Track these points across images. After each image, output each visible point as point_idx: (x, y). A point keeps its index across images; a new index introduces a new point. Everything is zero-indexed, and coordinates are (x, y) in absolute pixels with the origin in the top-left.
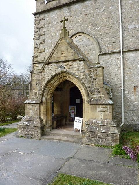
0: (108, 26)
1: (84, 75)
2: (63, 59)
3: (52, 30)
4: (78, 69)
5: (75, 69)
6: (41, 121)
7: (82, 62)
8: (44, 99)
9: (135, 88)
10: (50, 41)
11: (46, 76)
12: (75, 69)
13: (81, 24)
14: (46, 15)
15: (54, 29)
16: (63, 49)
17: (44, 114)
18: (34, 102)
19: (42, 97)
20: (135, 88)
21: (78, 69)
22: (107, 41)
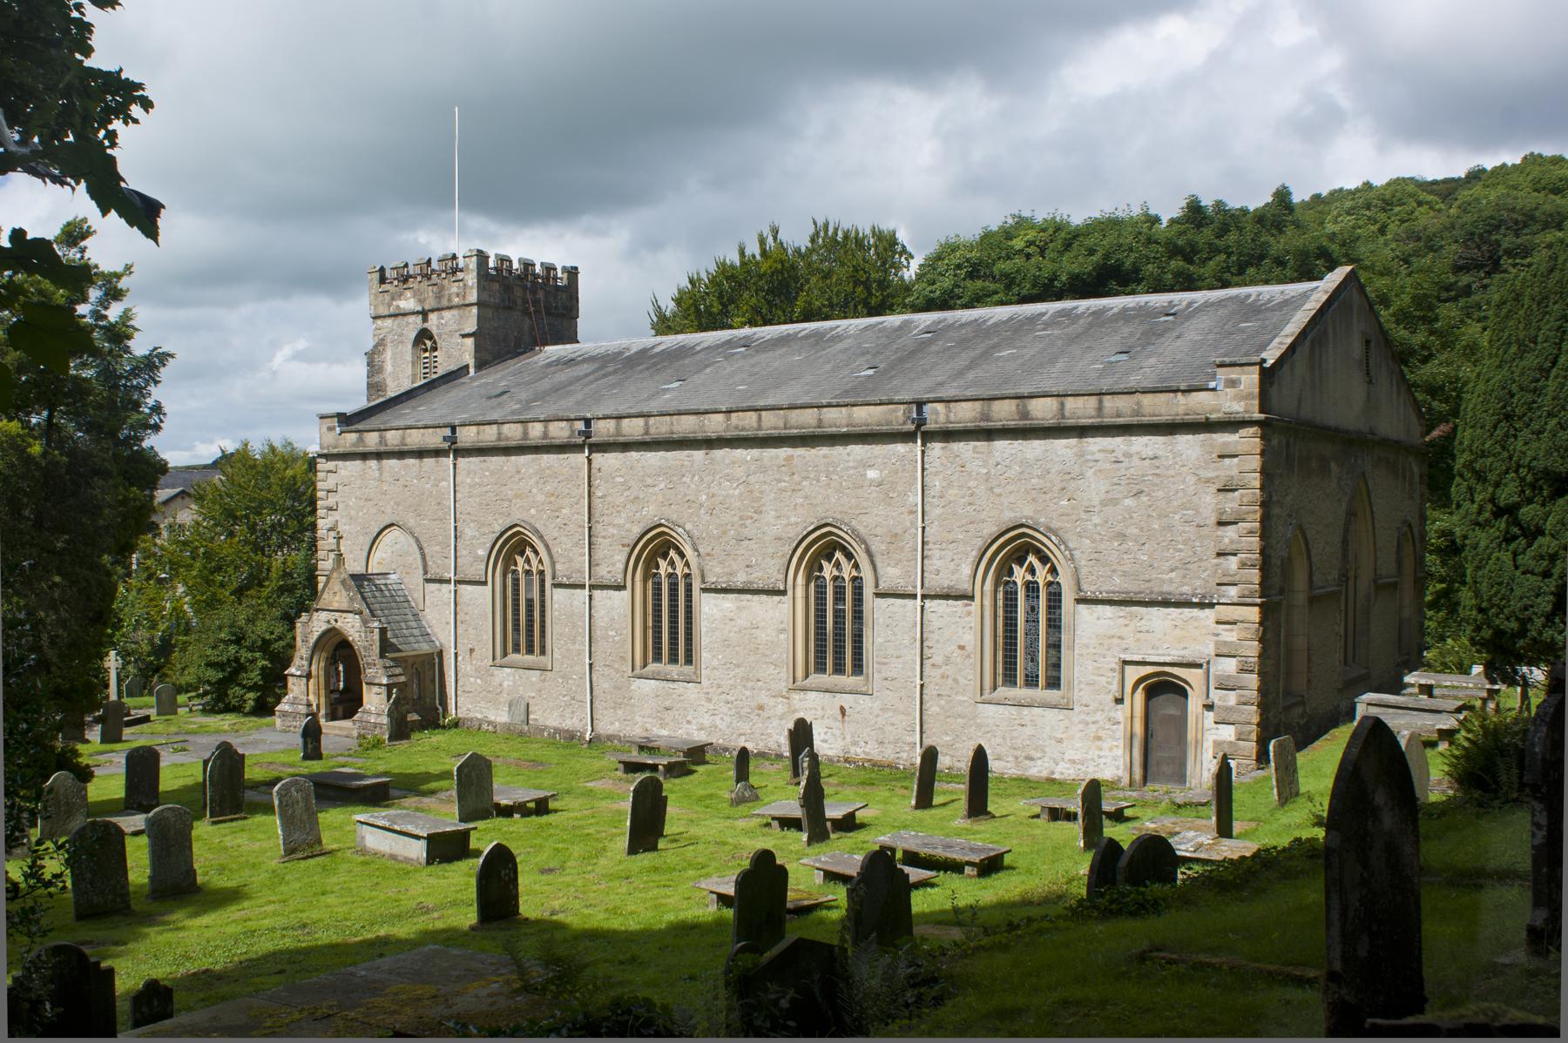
0: (438, 522)
1: (360, 636)
4: (353, 627)
5: (350, 625)
6: (309, 705)
7: (357, 616)
8: (314, 668)
9: (472, 650)
11: (314, 629)
12: (350, 625)
13: (398, 504)
17: (314, 693)
19: (310, 664)
20: (472, 650)
21: (353, 627)
22: (437, 552)
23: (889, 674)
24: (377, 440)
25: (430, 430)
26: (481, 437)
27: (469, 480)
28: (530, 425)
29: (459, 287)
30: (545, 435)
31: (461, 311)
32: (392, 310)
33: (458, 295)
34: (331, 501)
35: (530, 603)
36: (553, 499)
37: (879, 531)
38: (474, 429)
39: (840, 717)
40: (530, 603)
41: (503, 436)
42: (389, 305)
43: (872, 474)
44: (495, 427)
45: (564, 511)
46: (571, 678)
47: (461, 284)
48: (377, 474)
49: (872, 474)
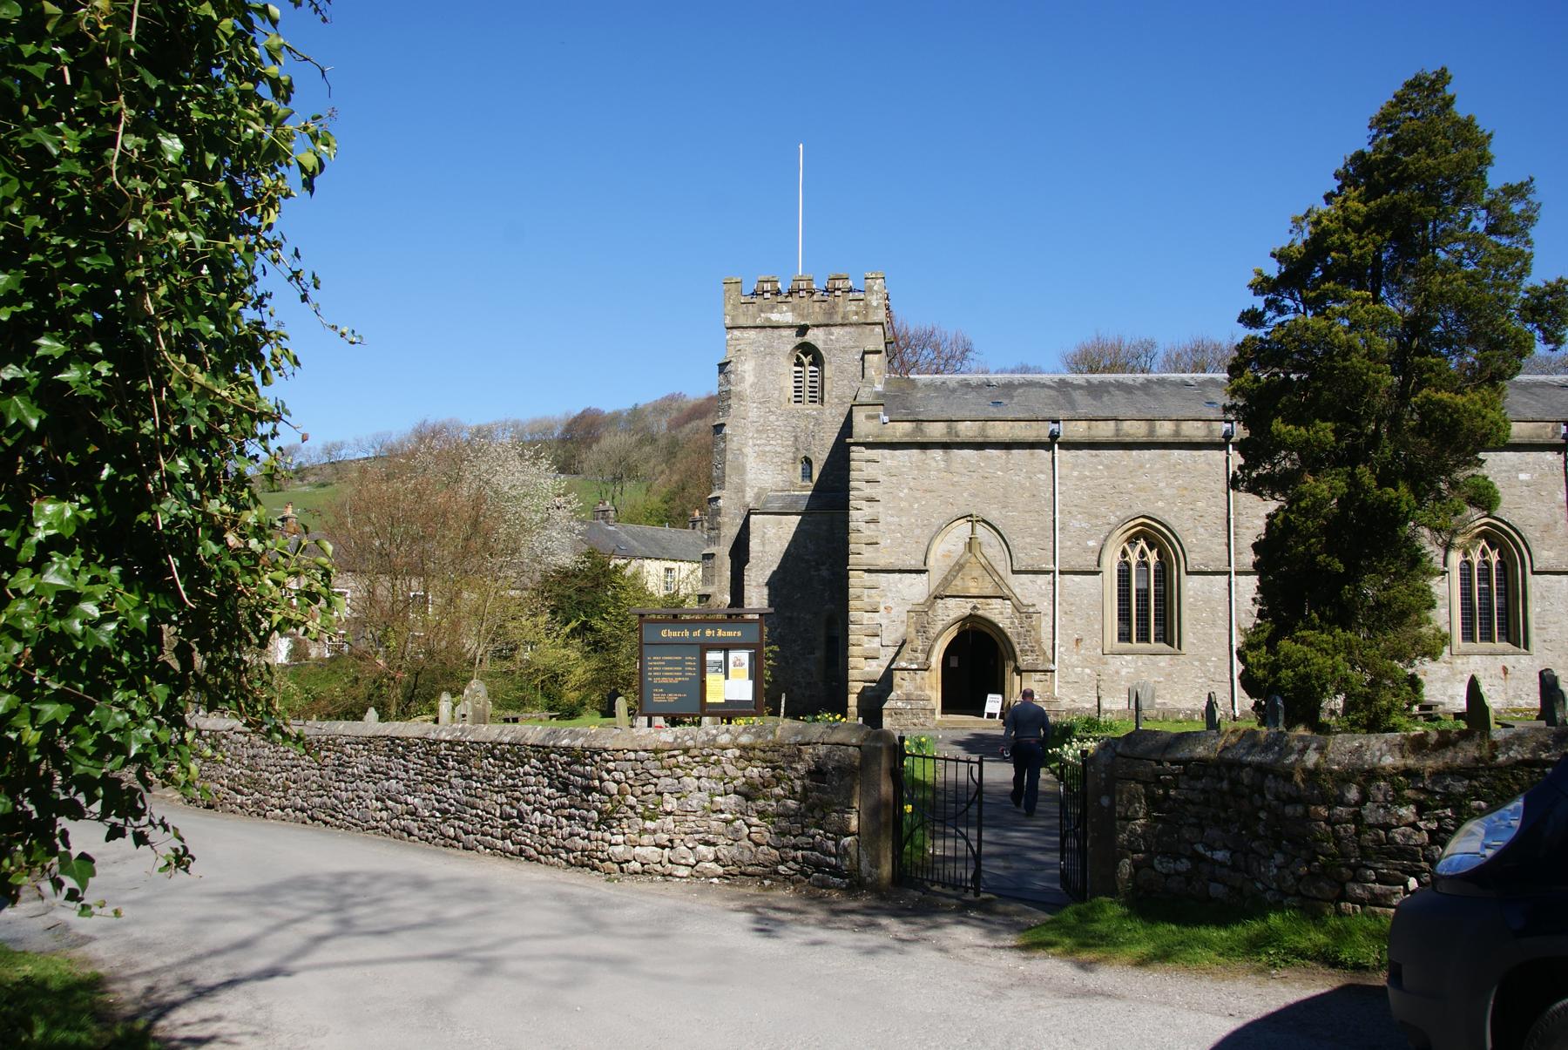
1: (1012, 623)
2: (974, 592)
3: (901, 495)
4: (1001, 613)
10: (896, 519)
14: (886, 452)
15: (906, 491)
16: (975, 574)
18: (915, 666)
23: (1547, 637)
24: (945, 431)
25: (1023, 424)
26: (1093, 433)
27: (1076, 474)
28: (1158, 423)
29: (858, 306)
30: (1177, 433)
31: (860, 330)
32: (759, 322)
33: (857, 313)
34: (868, 490)
35: (1143, 595)
36: (1185, 492)
37: (1531, 521)
38: (1084, 424)
39: (1502, 675)
40: (1143, 595)
41: (1122, 433)
42: (755, 318)
43: (1523, 476)
44: (1112, 423)
45: (1199, 504)
46: (1210, 661)
47: (861, 303)
48: (942, 464)
49: (1523, 476)
